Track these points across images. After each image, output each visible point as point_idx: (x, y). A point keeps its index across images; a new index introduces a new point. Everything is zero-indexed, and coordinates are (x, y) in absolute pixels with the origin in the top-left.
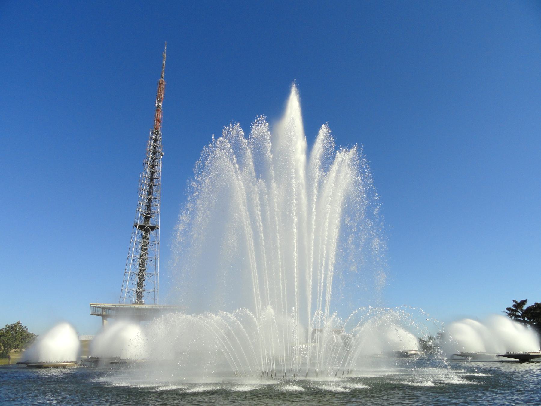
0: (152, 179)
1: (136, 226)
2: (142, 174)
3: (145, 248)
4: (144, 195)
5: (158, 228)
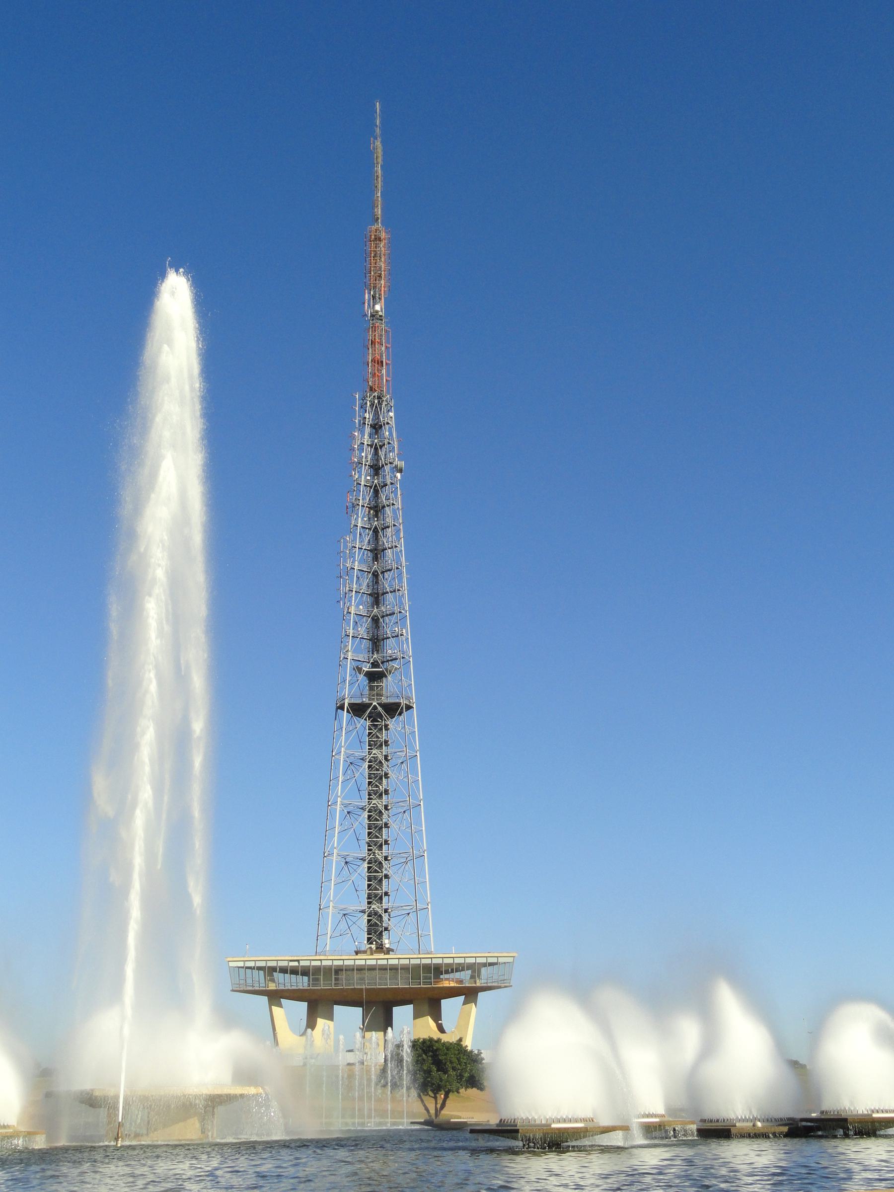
0: (377, 553)
1: (342, 707)
2: (346, 542)
3: (377, 775)
4: (357, 607)
5: (409, 707)
